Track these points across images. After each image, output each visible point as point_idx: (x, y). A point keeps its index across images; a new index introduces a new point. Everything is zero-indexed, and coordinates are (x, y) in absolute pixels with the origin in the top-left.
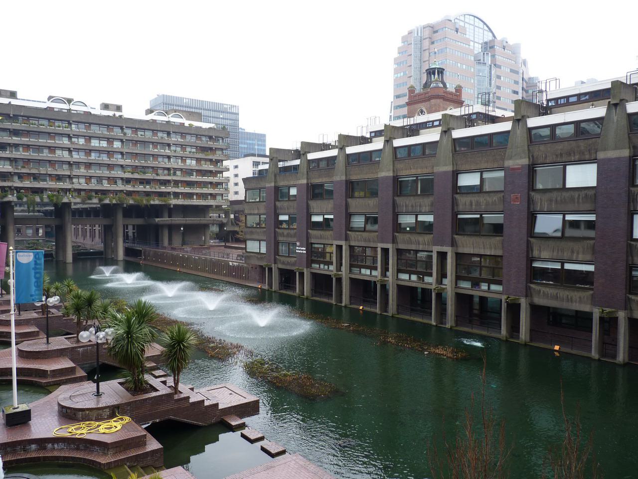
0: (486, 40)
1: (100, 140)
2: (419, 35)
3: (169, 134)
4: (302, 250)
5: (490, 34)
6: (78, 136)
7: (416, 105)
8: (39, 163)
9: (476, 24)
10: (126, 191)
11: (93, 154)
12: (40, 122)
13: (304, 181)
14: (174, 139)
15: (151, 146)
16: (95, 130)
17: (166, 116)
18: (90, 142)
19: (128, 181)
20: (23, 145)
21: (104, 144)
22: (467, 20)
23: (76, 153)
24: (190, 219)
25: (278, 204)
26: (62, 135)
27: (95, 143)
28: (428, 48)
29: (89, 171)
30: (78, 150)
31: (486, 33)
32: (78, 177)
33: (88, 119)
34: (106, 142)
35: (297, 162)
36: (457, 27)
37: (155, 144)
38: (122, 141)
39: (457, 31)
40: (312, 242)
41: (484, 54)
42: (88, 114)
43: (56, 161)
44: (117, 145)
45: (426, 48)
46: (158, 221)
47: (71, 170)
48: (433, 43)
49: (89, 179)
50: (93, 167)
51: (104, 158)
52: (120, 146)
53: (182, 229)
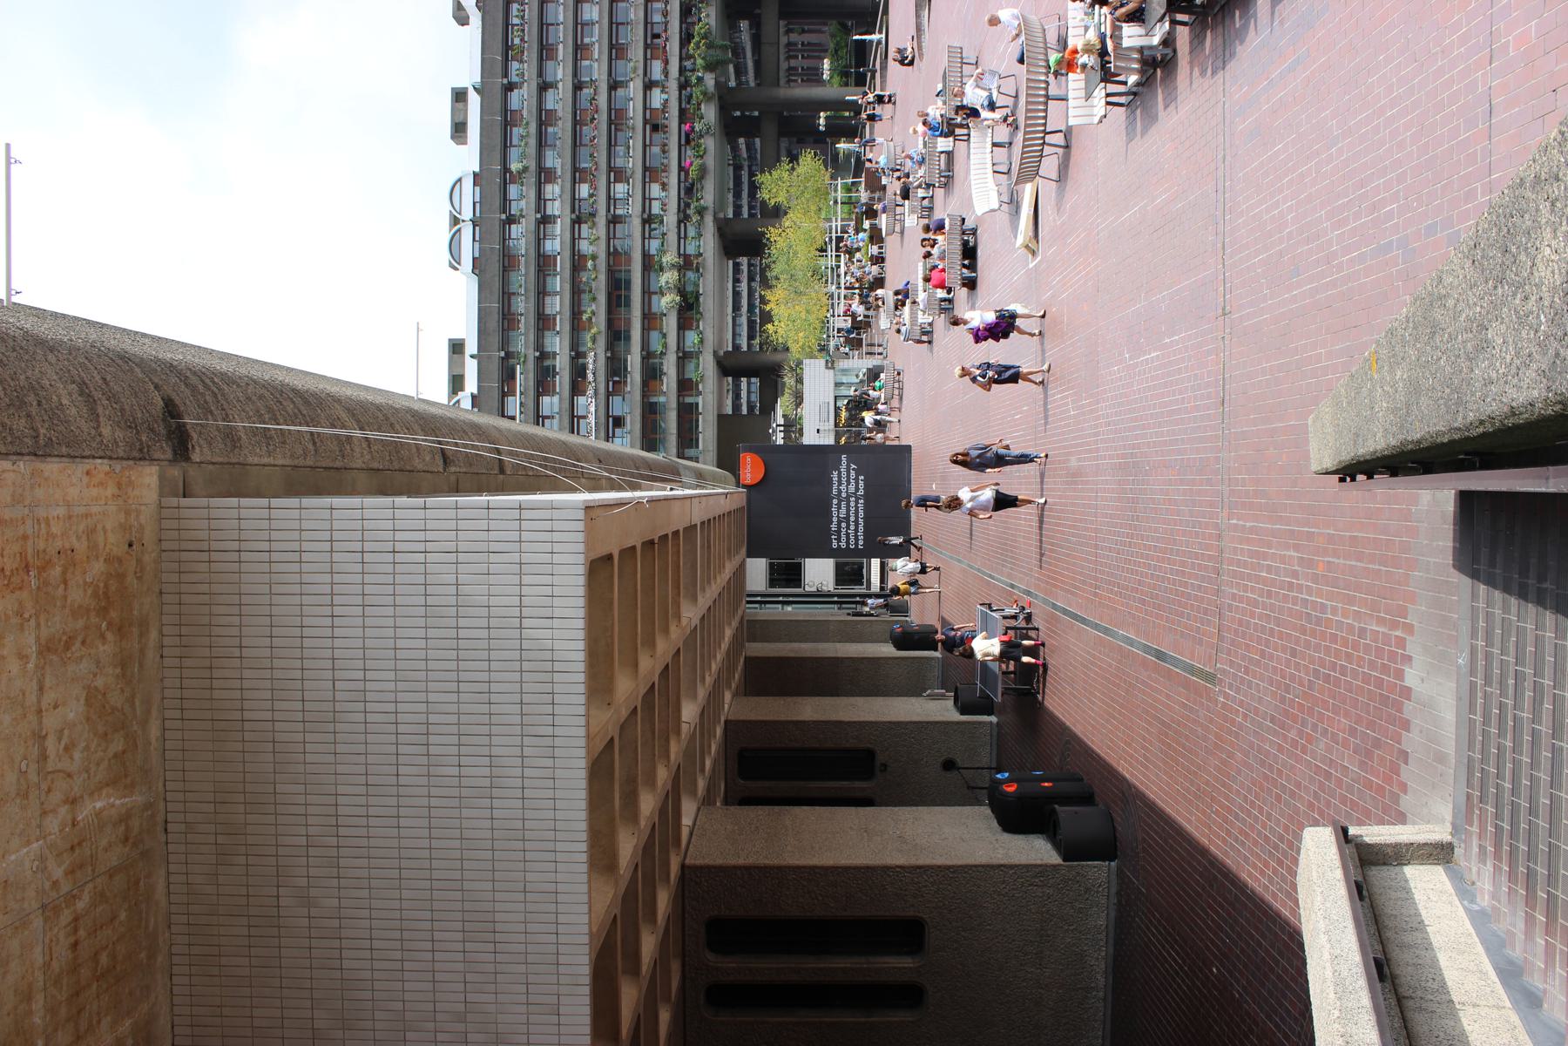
12: (516, 21)
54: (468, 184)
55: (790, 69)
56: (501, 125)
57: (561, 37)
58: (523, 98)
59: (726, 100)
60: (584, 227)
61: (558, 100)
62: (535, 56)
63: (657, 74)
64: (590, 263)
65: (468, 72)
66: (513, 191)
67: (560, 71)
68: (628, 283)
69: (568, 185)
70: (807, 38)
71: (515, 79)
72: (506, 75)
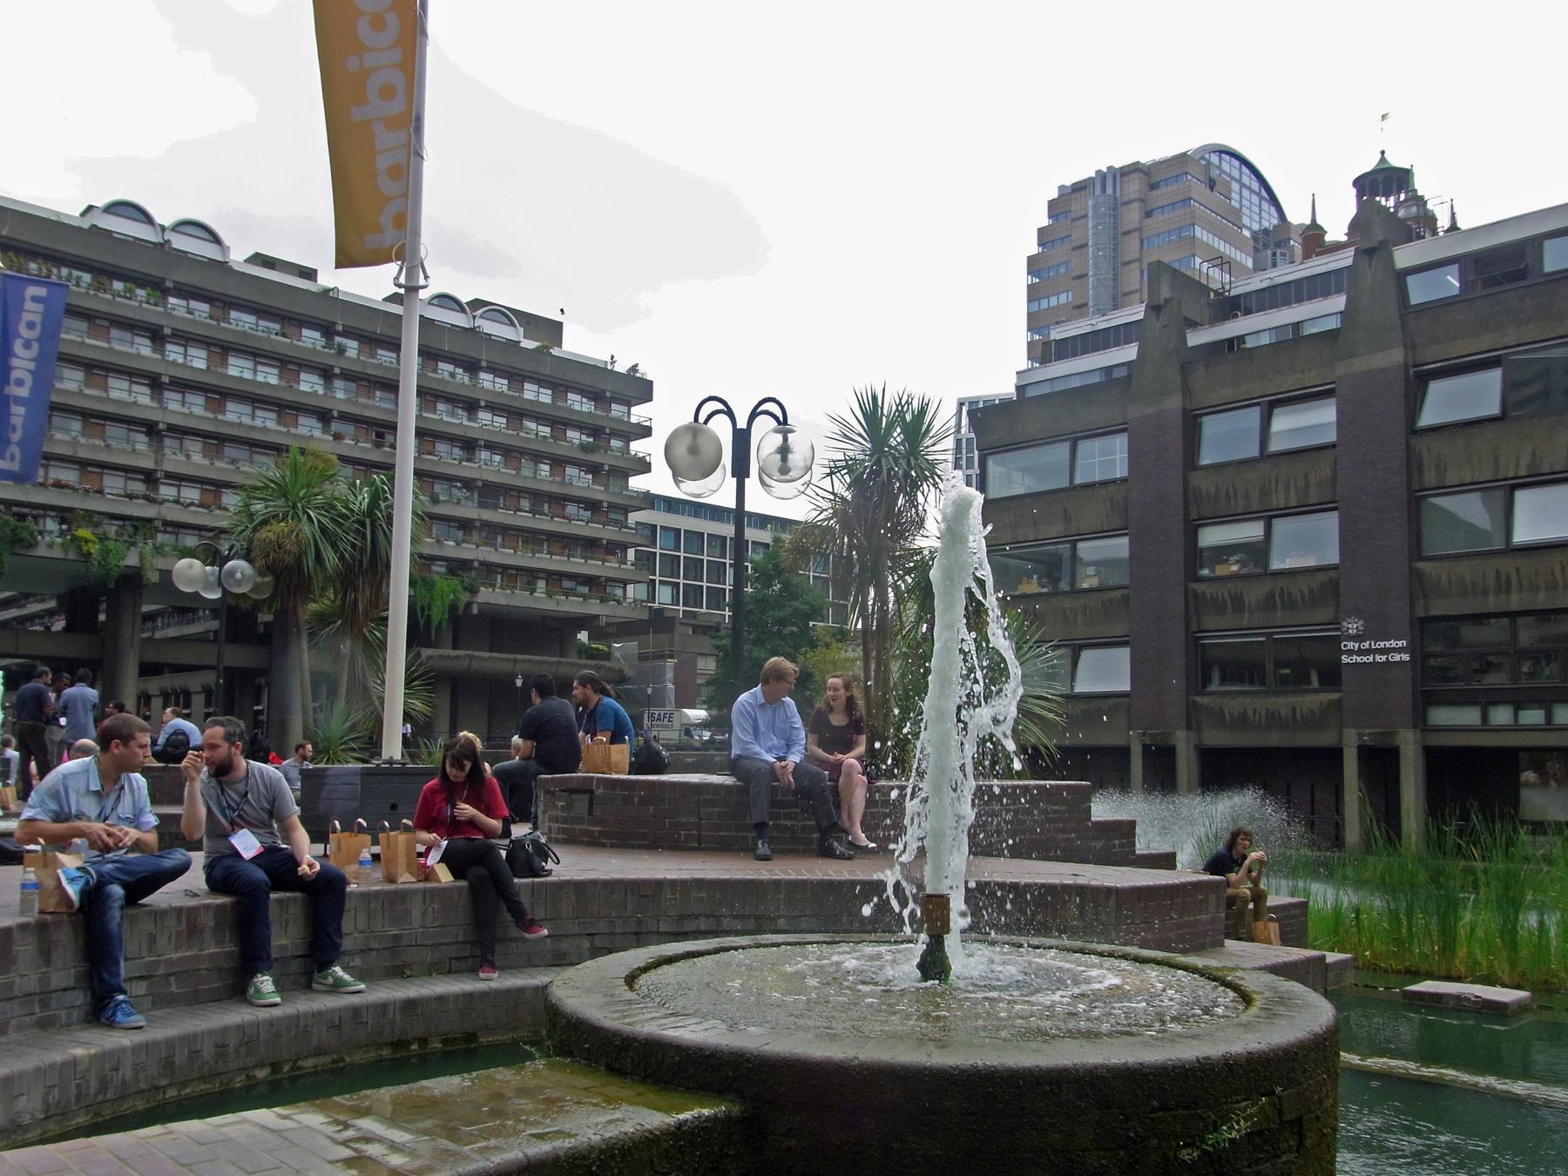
0: (1266, 224)
1: (257, 363)
2: (1109, 191)
3: (472, 367)
5: (1273, 210)
6: (186, 338)
9: (1246, 180)
11: (230, 406)
16: (242, 321)
18: (225, 364)
21: (269, 376)
22: (1225, 167)
23: (178, 396)
24: (528, 657)
27: (238, 369)
28: (1136, 225)
29: (218, 464)
30: (183, 386)
31: (1265, 206)
32: (178, 479)
36: (1215, 173)
38: (327, 374)
39: (1212, 188)
40: (1434, 612)
41: (1274, 254)
42: (223, 267)
44: (309, 384)
45: (1131, 227)
46: (430, 658)
47: (159, 451)
48: (1149, 214)
52: (321, 392)
53: (519, 683)
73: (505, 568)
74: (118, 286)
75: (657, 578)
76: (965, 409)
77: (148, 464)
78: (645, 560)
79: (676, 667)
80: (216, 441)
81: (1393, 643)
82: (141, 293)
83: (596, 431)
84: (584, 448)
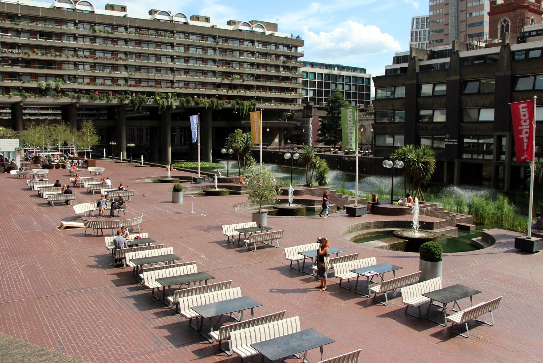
3: (253, 42)
4: (453, 142)
6: (179, 45)
7: (498, 15)
8: (148, 69)
10: (218, 95)
11: (191, 61)
12: (150, 32)
13: (457, 78)
14: (258, 47)
15: (238, 53)
17: (250, 26)
19: (218, 86)
20: (135, 53)
21: (200, 51)
25: (420, 100)
26: (166, 44)
32: (179, 82)
33: (187, 31)
34: (201, 50)
35: (447, 60)
37: (241, 52)
38: (214, 49)
43: (161, 67)
44: (210, 52)
46: (244, 123)
49: (187, 84)
50: (191, 73)
51: (200, 66)
53: (268, 130)
54: (89, 9)
55: (134, 129)
56: (113, 24)
57: (144, 49)
58: (121, 33)
59: (121, 107)
60: (72, 53)
61: (121, 47)
62: (137, 38)
63: (130, 82)
64: (58, 54)
65: (131, 13)
66: (87, 26)
67: (130, 48)
68: (51, 68)
69: (89, 47)
70: (145, 136)
71: (129, 30)
72: (131, 27)
73: (263, 98)
74: (163, 33)
75: (309, 88)
76: (415, 21)
77: (171, 79)
78: (305, 83)
79: (312, 120)
80: (187, 71)
81: (454, 140)
82: (168, 35)
83: (288, 57)
84: (284, 62)
